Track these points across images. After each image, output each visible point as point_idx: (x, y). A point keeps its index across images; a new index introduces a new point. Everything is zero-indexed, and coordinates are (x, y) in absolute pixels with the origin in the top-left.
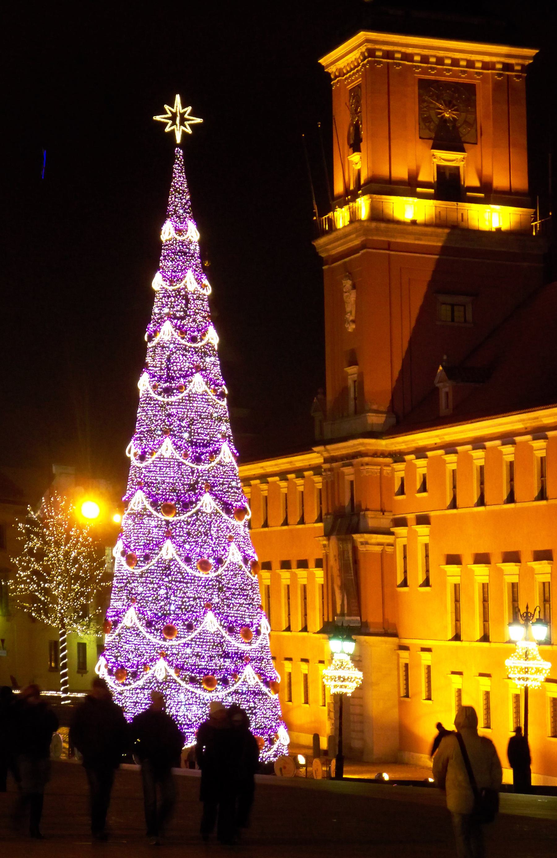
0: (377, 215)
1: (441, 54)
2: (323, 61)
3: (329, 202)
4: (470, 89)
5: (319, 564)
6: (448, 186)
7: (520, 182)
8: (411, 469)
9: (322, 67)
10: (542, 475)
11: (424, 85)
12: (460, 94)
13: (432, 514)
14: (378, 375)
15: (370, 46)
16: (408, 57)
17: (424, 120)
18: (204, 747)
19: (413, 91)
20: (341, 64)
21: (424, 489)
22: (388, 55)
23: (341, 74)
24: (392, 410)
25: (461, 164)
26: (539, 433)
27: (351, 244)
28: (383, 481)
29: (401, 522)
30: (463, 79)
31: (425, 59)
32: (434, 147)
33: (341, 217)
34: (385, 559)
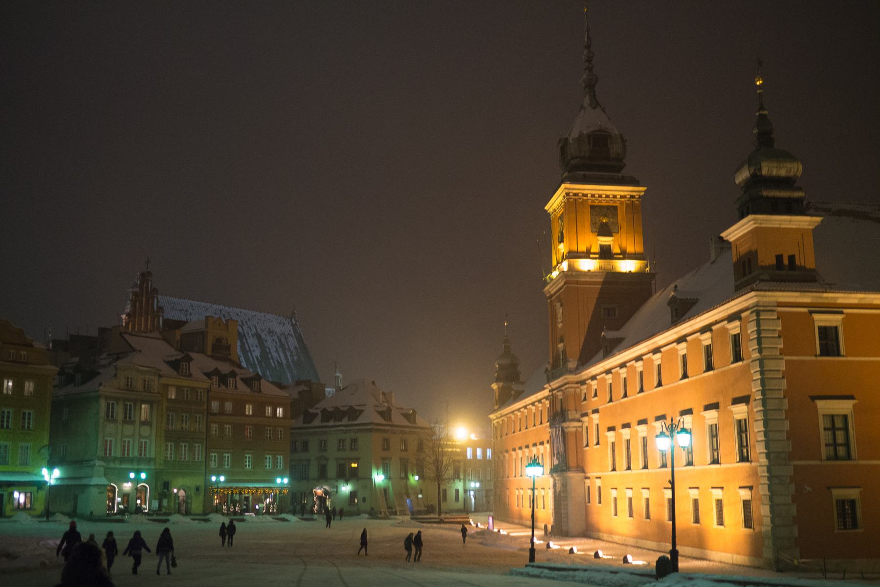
0: (570, 267)
1: (601, 192)
2: (546, 208)
3: (550, 270)
4: (615, 208)
5: (548, 442)
6: (605, 253)
7: (639, 249)
8: (590, 386)
9: (546, 211)
10: (659, 374)
11: (593, 207)
12: (611, 210)
13: (600, 408)
14: (574, 346)
15: (567, 191)
16: (586, 195)
17: (593, 224)
18: (214, 479)
19: (588, 210)
20: (554, 206)
21: (596, 395)
22: (576, 195)
23: (555, 210)
24: (580, 359)
25: (611, 243)
26: (656, 351)
27: (560, 286)
28: (576, 396)
29: (586, 415)
30: (611, 204)
31: (593, 196)
32: (598, 235)
33: (555, 274)
34: (578, 435)
